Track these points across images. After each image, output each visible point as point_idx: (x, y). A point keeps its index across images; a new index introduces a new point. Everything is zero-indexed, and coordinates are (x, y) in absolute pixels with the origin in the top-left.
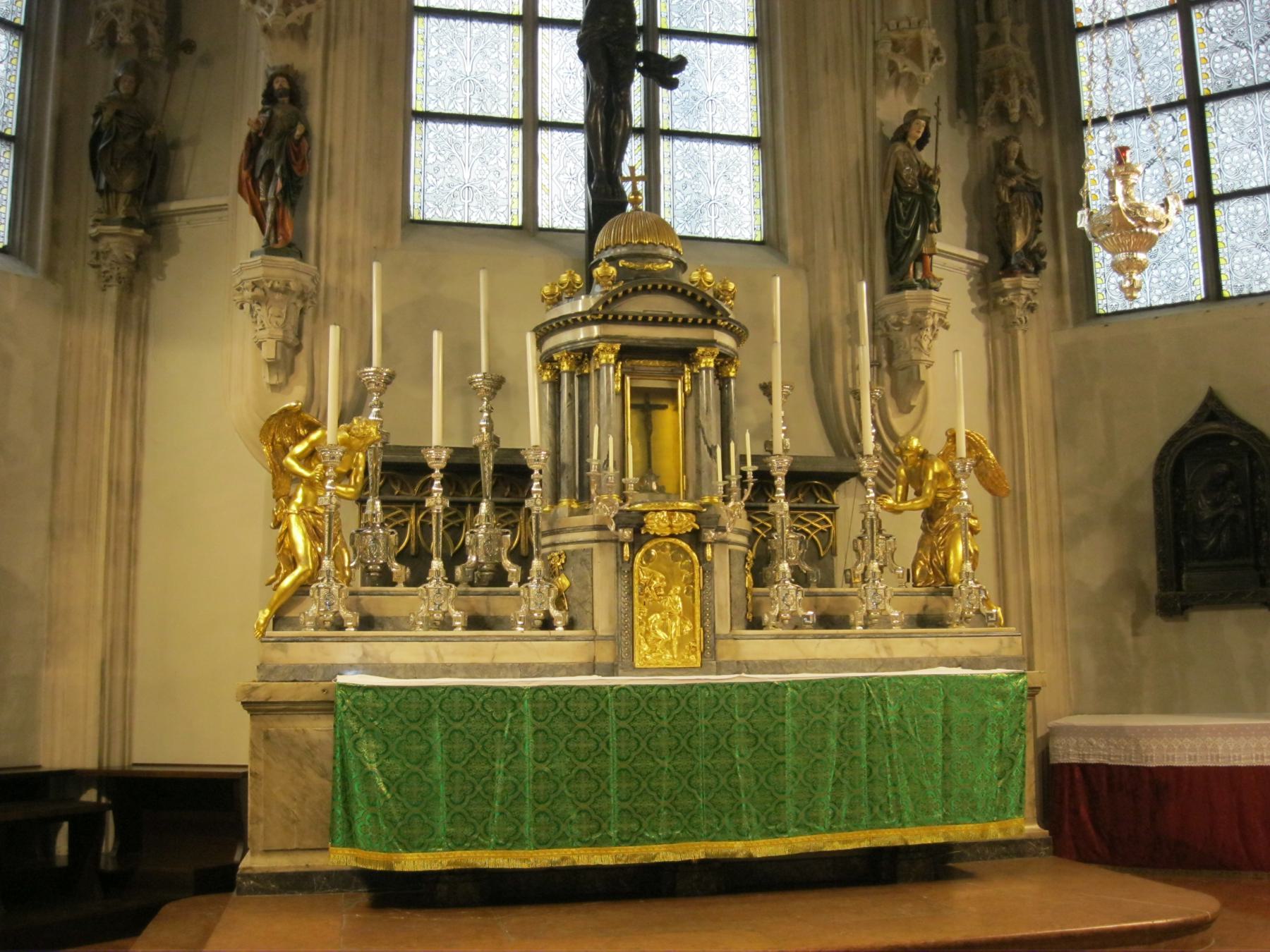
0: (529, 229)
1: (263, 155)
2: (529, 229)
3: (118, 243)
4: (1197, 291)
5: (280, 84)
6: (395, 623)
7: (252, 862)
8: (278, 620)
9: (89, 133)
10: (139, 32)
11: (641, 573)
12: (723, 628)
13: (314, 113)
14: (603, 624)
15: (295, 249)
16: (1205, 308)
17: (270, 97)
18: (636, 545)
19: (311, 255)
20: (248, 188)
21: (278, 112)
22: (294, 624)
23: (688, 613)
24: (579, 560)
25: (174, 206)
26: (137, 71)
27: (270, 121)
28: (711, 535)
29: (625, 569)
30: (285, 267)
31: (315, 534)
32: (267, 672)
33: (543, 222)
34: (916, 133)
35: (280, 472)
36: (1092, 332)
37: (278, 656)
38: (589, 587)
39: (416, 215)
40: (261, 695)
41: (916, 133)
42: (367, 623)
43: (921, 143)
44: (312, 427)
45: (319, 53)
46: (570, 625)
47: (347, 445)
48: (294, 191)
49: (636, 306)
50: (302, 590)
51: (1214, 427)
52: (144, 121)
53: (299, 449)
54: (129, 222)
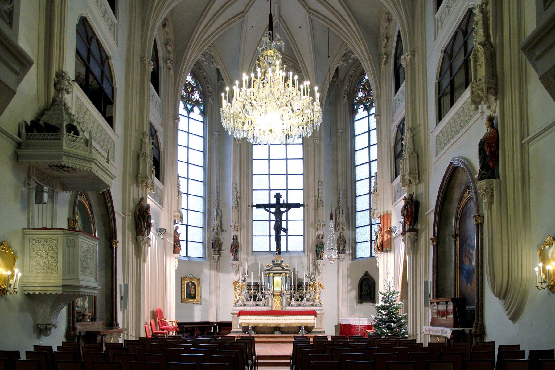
0: (270, 251)
1: (233, 247)
2: (270, 251)
3: (216, 257)
4: (369, 255)
5: (235, 237)
6: (248, 305)
7: (233, 330)
8: (235, 304)
9: (212, 243)
10: (217, 229)
11: (274, 300)
12: (284, 306)
13: (239, 240)
14: (270, 305)
15: (237, 260)
16: (369, 258)
17: (233, 239)
18: (274, 296)
19: (239, 259)
20: (232, 251)
21: (234, 241)
22: (237, 305)
23: (280, 304)
24: (268, 298)
25: (221, 251)
26: (217, 234)
27: (233, 243)
28: (282, 295)
29: (272, 299)
30: (235, 262)
31: (239, 295)
32: (234, 310)
33: (271, 250)
34: (321, 237)
35: (235, 288)
36: (357, 261)
37: (235, 308)
38: (269, 301)
39: (254, 250)
40: (233, 313)
41: (321, 237)
42: (245, 305)
43: (322, 238)
44: (239, 283)
45: (240, 232)
46: (267, 305)
47: (242, 285)
48: (237, 251)
49: (274, 269)
50: (237, 302)
51: (366, 277)
52: (219, 240)
53: (237, 285)
54: (217, 254)
